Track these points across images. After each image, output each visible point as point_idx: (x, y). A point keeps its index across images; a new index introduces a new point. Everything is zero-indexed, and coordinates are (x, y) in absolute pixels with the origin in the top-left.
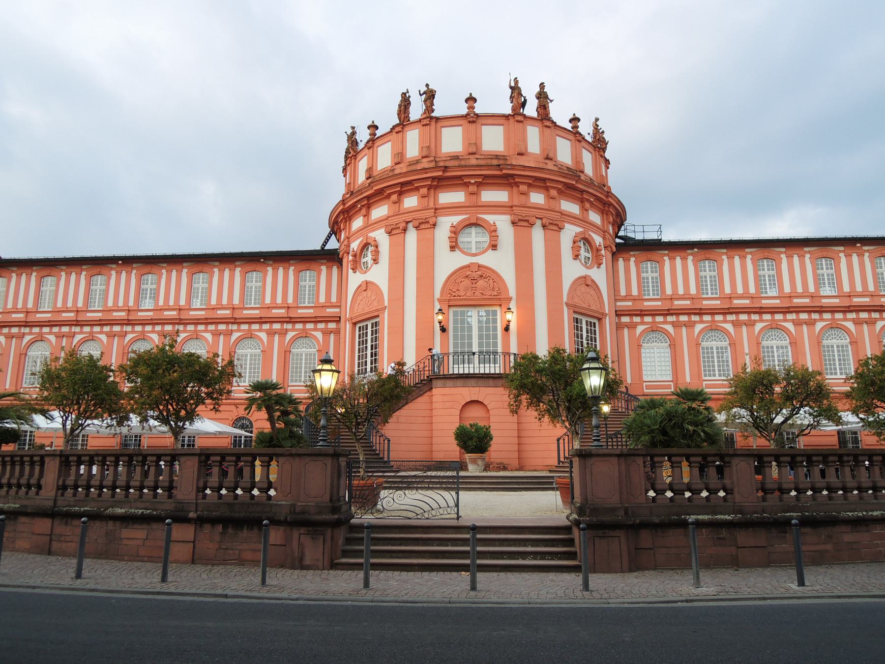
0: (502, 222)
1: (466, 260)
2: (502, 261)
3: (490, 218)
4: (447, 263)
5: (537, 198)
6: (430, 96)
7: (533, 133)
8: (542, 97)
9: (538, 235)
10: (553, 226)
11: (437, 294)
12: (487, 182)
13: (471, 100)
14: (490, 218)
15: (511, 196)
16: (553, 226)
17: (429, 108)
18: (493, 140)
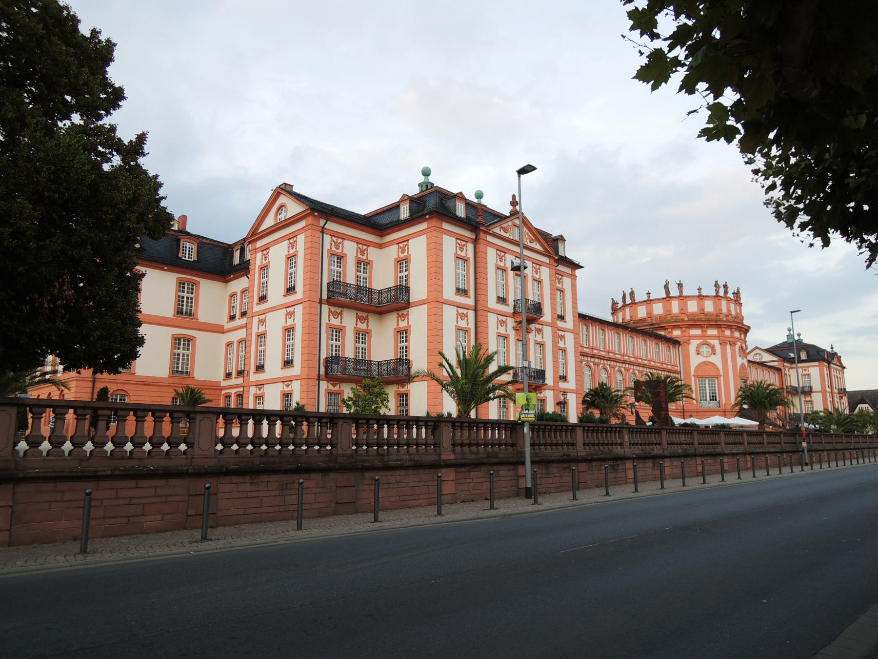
0: (716, 343)
1: (704, 359)
2: (717, 360)
3: (712, 342)
4: (695, 360)
5: (728, 333)
6: (680, 286)
7: (724, 303)
8: (725, 286)
9: (728, 347)
10: (733, 344)
11: (692, 373)
12: (711, 326)
13: (699, 289)
14: (712, 342)
15: (718, 332)
16: (733, 344)
17: (681, 292)
18: (709, 306)
